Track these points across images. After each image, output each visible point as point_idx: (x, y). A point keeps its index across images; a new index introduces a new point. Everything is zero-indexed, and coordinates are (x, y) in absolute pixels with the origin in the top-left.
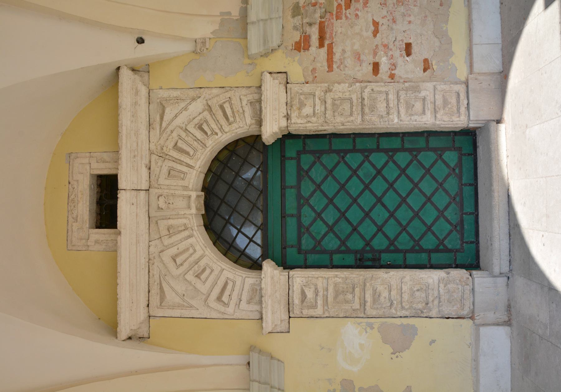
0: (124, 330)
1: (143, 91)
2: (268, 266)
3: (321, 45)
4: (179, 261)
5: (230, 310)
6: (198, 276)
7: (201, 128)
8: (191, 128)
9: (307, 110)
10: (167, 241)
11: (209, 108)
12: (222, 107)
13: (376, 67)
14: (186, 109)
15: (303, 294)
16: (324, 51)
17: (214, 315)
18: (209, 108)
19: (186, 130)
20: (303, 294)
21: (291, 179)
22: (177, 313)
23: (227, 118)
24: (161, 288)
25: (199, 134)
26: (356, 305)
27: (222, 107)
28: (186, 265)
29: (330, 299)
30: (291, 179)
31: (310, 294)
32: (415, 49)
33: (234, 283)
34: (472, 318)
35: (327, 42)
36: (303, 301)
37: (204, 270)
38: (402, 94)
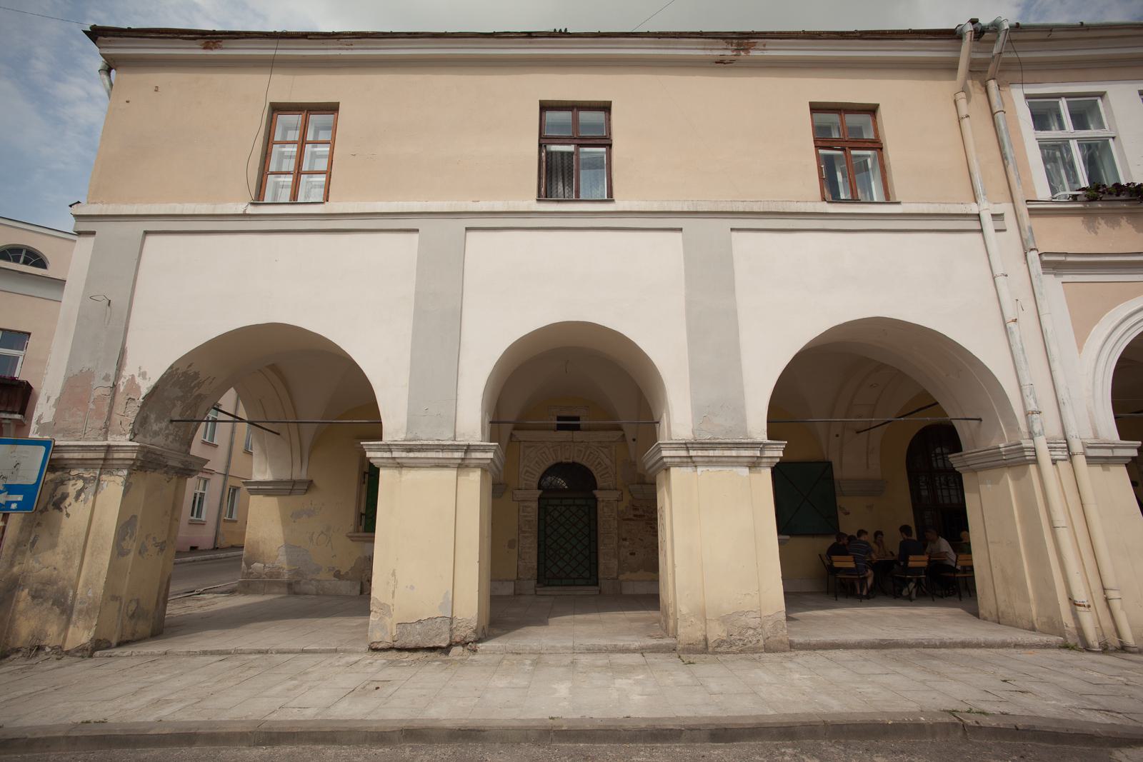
0: (515, 433)
1: (614, 440)
2: (540, 492)
3: (635, 516)
4: (544, 455)
5: (523, 476)
6: (537, 462)
7: (599, 463)
8: (599, 459)
9: (606, 509)
10: (551, 450)
11: (607, 468)
12: (608, 472)
13: (625, 540)
14: (607, 457)
15: (529, 507)
16: (631, 516)
17: (521, 469)
18: (607, 468)
19: (597, 458)
20: (529, 507)
21: (578, 502)
22: (522, 454)
23: (603, 475)
24: (531, 447)
25: (596, 463)
26: (523, 529)
27: (608, 472)
28: (541, 457)
29: (527, 519)
30: (578, 502)
31: (529, 509)
32: (632, 556)
33: (533, 478)
34: (517, 579)
35: (634, 518)
36: (526, 507)
37: (539, 465)
38: (613, 550)
